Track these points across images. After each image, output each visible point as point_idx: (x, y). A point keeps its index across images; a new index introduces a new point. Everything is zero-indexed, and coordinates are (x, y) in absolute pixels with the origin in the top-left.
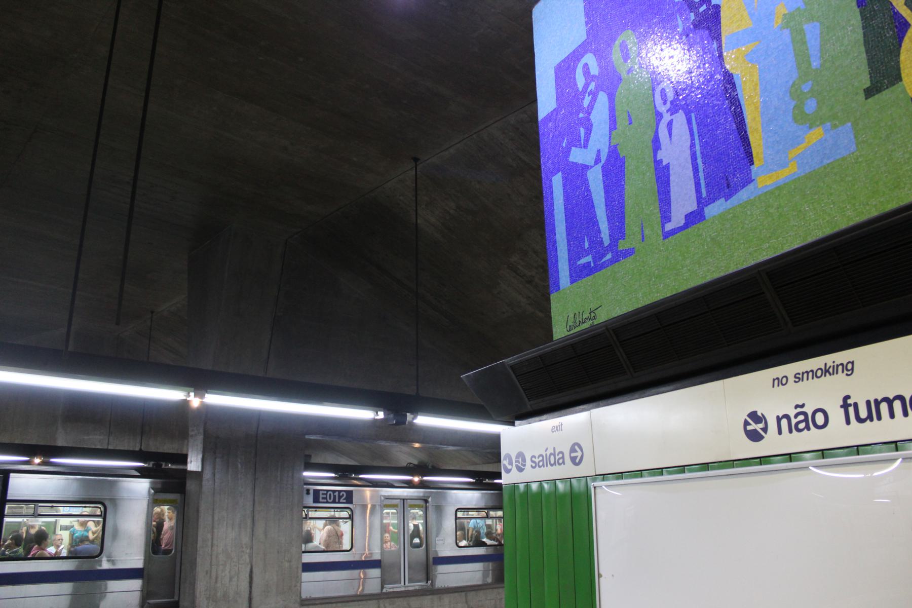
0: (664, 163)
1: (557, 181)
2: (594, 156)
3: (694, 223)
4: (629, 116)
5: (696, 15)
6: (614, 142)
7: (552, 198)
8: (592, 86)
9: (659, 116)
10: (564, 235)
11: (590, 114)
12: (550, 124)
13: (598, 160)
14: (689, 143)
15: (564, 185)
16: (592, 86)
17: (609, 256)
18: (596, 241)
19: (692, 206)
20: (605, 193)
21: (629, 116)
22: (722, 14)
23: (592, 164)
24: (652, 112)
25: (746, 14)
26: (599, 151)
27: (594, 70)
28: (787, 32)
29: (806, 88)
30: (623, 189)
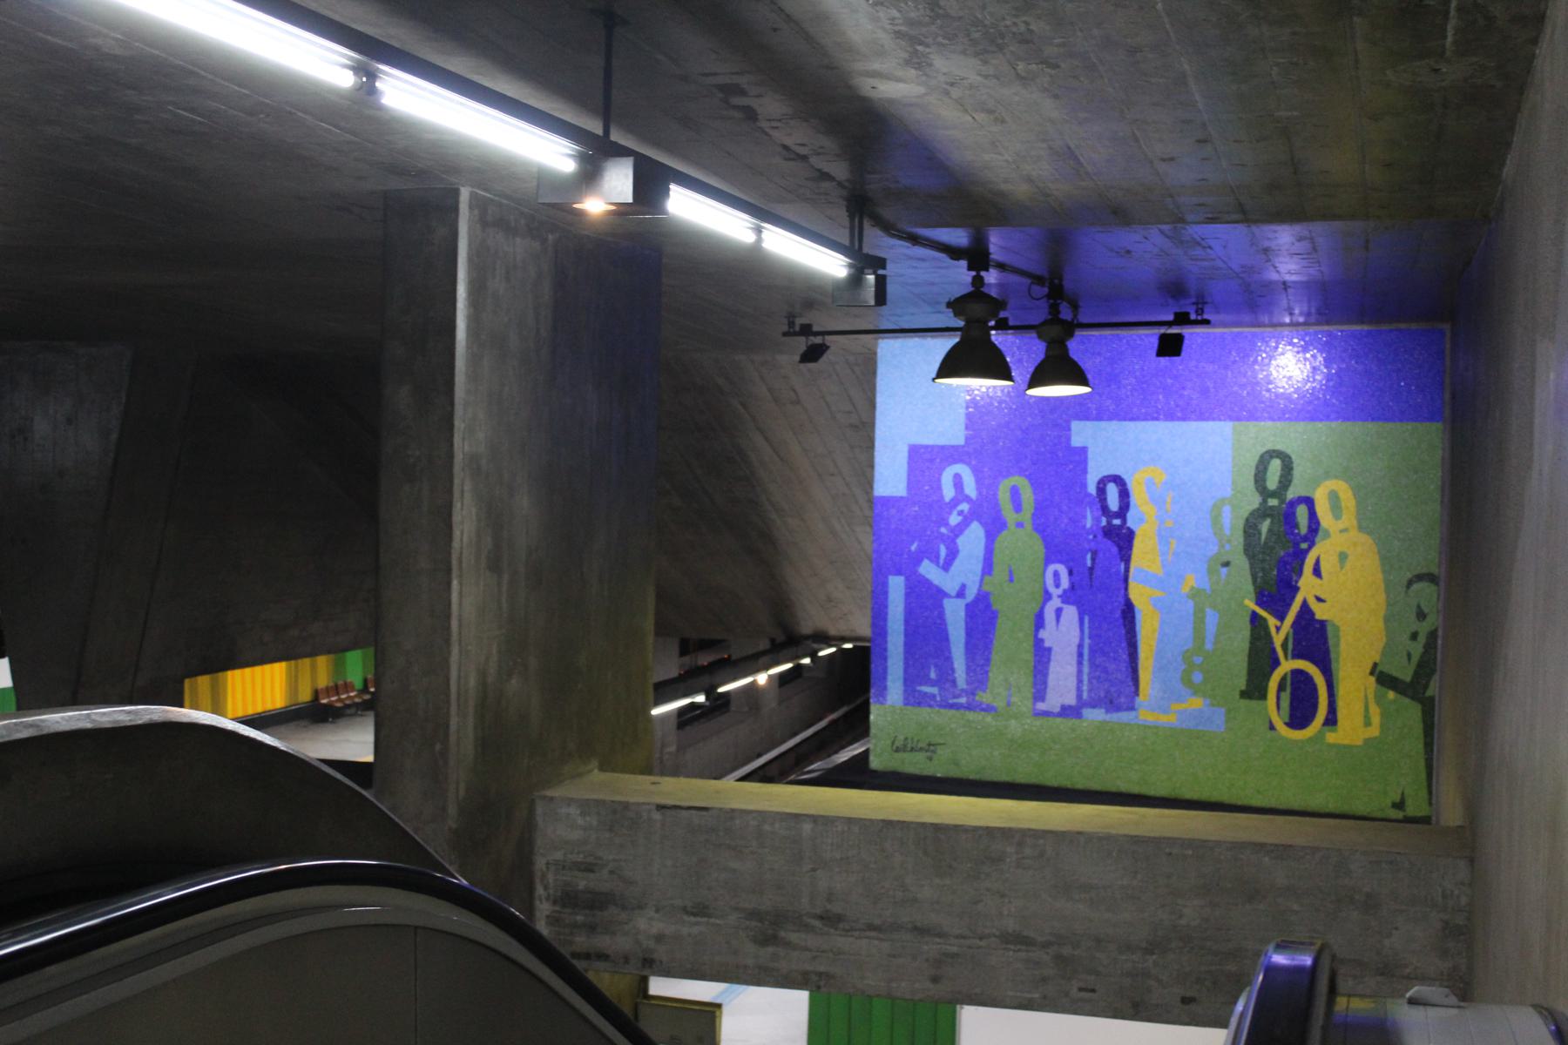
0: (1047, 644)
1: (896, 586)
4: (1011, 572)
5: (1109, 523)
6: (986, 588)
8: (965, 507)
9: (1047, 596)
10: (901, 649)
11: (957, 536)
12: (893, 511)
13: (961, 594)
14: (1076, 641)
15: (907, 595)
16: (965, 507)
17: (963, 700)
18: (946, 677)
19: (1071, 700)
21: (1011, 572)
22: (1137, 543)
23: (953, 593)
24: (1042, 592)
26: (963, 588)
27: (970, 489)
28: (1191, 603)
29: (1198, 660)
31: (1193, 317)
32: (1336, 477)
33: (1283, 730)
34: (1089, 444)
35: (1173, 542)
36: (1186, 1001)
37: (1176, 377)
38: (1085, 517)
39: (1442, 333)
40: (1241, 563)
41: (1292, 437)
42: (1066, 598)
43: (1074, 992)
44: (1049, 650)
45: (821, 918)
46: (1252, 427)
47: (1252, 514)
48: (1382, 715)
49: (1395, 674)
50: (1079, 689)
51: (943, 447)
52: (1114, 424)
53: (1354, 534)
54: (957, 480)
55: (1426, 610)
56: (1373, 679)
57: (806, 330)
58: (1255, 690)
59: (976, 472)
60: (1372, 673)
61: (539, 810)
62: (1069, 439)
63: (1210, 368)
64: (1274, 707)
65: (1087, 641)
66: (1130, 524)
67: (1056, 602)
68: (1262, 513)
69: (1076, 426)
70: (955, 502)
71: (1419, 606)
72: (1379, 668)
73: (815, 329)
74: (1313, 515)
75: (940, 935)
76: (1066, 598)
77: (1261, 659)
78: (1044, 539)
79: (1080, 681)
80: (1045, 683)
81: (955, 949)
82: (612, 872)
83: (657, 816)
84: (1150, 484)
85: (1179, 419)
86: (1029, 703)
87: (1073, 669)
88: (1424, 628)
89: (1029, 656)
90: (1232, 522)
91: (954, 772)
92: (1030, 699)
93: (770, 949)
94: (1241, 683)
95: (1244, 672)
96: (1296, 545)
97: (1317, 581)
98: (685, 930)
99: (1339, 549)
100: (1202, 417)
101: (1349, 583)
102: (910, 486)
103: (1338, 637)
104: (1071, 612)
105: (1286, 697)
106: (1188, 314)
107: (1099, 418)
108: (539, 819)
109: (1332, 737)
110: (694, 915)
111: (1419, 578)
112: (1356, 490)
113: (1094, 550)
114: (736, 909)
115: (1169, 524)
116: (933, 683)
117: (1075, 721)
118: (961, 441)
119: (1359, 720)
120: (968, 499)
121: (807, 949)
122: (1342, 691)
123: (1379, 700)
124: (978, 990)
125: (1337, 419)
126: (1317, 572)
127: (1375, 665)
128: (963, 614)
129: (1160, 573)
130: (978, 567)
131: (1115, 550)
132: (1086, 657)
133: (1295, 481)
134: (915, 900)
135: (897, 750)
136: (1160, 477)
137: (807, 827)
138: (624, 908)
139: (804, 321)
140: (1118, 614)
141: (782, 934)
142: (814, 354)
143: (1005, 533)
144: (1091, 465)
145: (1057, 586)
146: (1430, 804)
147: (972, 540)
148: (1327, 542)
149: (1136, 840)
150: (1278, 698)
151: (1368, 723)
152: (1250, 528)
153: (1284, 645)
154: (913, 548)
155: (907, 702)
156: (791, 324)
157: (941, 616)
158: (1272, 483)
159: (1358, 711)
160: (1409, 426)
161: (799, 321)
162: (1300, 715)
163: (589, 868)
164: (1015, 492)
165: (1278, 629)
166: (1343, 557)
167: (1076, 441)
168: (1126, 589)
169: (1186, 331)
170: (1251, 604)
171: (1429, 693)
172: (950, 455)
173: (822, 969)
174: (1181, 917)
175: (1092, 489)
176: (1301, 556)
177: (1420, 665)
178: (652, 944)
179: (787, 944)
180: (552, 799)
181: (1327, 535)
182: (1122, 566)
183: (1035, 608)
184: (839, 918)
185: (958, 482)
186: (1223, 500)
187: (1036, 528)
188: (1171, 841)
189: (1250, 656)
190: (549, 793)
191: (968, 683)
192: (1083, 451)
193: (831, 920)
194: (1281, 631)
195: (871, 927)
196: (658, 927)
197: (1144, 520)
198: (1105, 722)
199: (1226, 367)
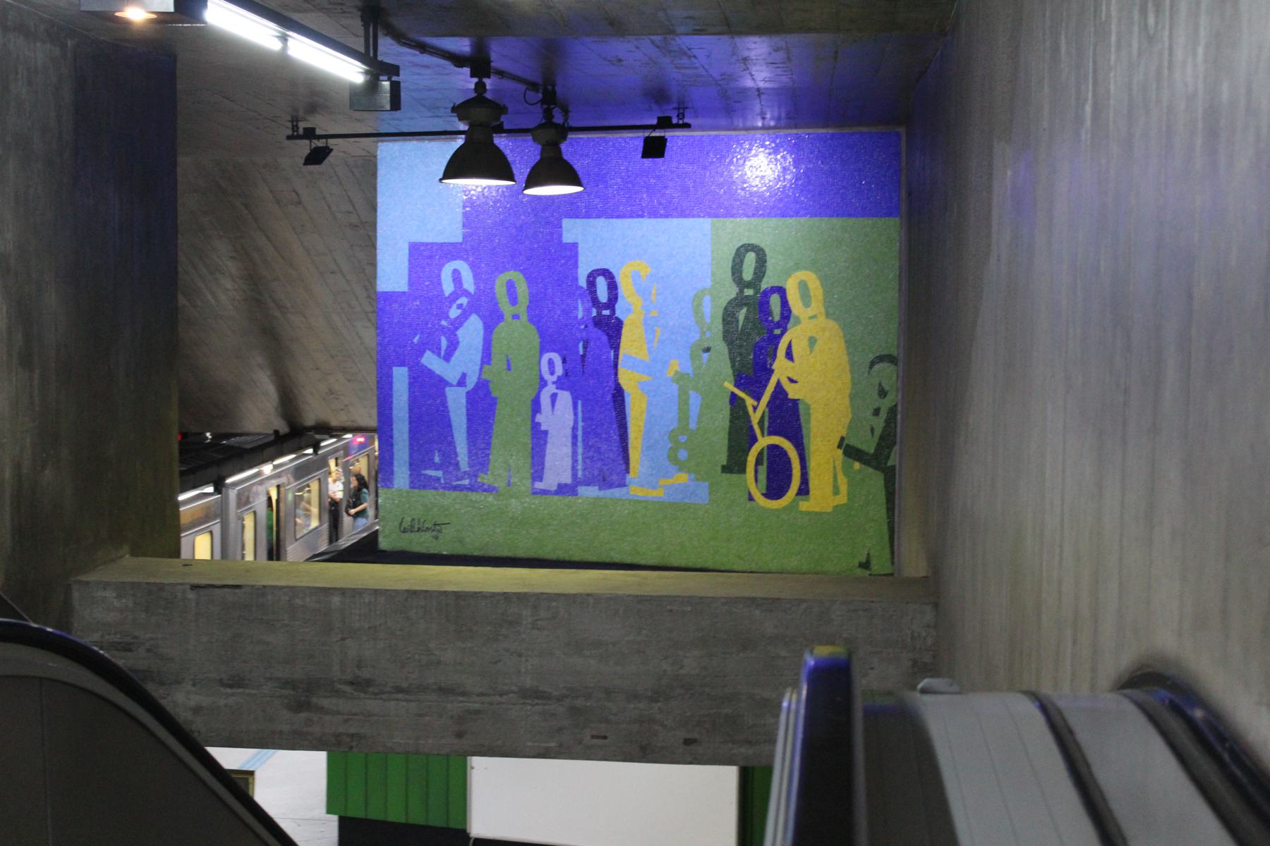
2: (458, 377)
3: (564, 494)
5: (599, 314)
6: (484, 376)
7: (391, 389)
8: (463, 301)
9: (543, 383)
10: (406, 436)
11: (457, 329)
12: (395, 306)
13: (462, 382)
14: (571, 424)
15: (411, 384)
16: (463, 301)
17: (466, 482)
18: (450, 460)
19: (569, 481)
20: (469, 420)
22: (625, 331)
23: (455, 383)
25: (645, 347)
26: (464, 376)
27: (469, 283)
28: (675, 386)
29: (683, 439)
30: (491, 427)
31: (675, 121)
32: (805, 268)
33: (761, 501)
34: (580, 240)
35: (659, 331)
36: (688, 742)
37: (658, 177)
38: (576, 308)
39: (898, 135)
40: (721, 348)
41: (763, 231)
42: (560, 384)
43: (587, 740)
44: (546, 433)
45: (352, 683)
46: (729, 222)
47: (730, 302)
48: (850, 485)
49: (859, 446)
50: (574, 468)
51: (442, 245)
52: (602, 221)
53: (822, 319)
54: (456, 275)
55: (887, 388)
56: (840, 452)
57: (310, 134)
58: (735, 465)
59: (474, 267)
60: (839, 446)
61: (76, 595)
62: (560, 236)
63: (689, 168)
64: (752, 480)
65: (580, 424)
66: (618, 314)
67: (551, 389)
68: (739, 302)
69: (567, 223)
70: (454, 297)
71: (880, 385)
72: (846, 442)
73: (318, 132)
74: (785, 303)
75: (464, 694)
76: (560, 384)
77: (741, 436)
78: (538, 328)
79: (575, 461)
80: (542, 464)
81: (477, 706)
82: (149, 650)
83: (191, 595)
84: (636, 276)
85: (662, 216)
86: (528, 482)
87: (568, 450)
88: (886, 404)
89: (528, 440)
90: (712, 311)
91: (459, 550)
92: (530, 480)
93: (303, 715)
94: (723, 459)
95: (725, 449)
96: (770, 331)
97: (789, 363)
98: (222, 702)
99: (809, 334)
100: (683, 214)
101: (819, 366)
102: (411, 284)
103: (809, 415)
104: (565, 397)
105: (763, 469)
106: (670, 118)
107: (588, 216)
108: (76, 604)
109: (804, 506)
110: (231, 686)
111: (881, 359)
112: (824, 280)
113: (587, 336)
114: (271, 679)
115: (654, 313)
116: (437, 467)
117: (569, 499)
118: (460, 240)
119: (829, 490)
120: (466, 293)
121: (338, 713)
122: (813, 464)
123: (847, 470)
124: (499, 743)
125: (805, 215)
126: (789, 355)
127: (842, 439)
128: (464, 401)
129: (647, 359)
130: (478, 357)
131: (605, 338)
132: (580, 439)
133: (768, 272)
134: (439, 662)
135: (404, 531)
136: (645, 270)
137: (336, 600)
138: (162, 684)
139: (309, 125)
140: (609, 398)
141: (314, 700)
142: (317, 156)
143: (502, 324)
144: (581, 259)
145: (552, 373)
146: (893, 563)
147: (471, 332)
148: (798, 327)
149: (641, 599)
150: (756, 471)
151: (836, 491)
152: (728, 316)
153: (761, 422)
154: (416, 340)
155: (413, 485)
156: (295, 128)
157: (444, 403)
158: (748, 275)
159: (828, 480)
160: (869, 221)
161: (302, 125)
162: (776, 489)
163: (127, 648)
164: (511, 286)
165: (755, 408)
166: (812, 341)
167: (567, 238)
168: (616, 374)
169: (668, 134)
170: (730, 386)
171: (890, 463)
172: (448, 252)
173: (352, 731)
174: (682, 667)
175: (583, 282)
176: (775, 340)
177: (882, 438)
178: (189, 716)
179: (321, 710)
180: (88, 583)
181: (798, 321)
182: (612, 353)
183: (529, 394)
184: (369, 683)
185: (457, 277)
186: (703, 291)
187: (531, 320)
188: (672, 599)
189: (730, 434)
190: (84, 578)
191: (471, 466)
192: (574, 246)
193: (361, 685)
194: (757, 410)
195: (399, 690)
196: (195, 700)
197: (631, 309)
198: (598, 498)
199: (705, 168)
